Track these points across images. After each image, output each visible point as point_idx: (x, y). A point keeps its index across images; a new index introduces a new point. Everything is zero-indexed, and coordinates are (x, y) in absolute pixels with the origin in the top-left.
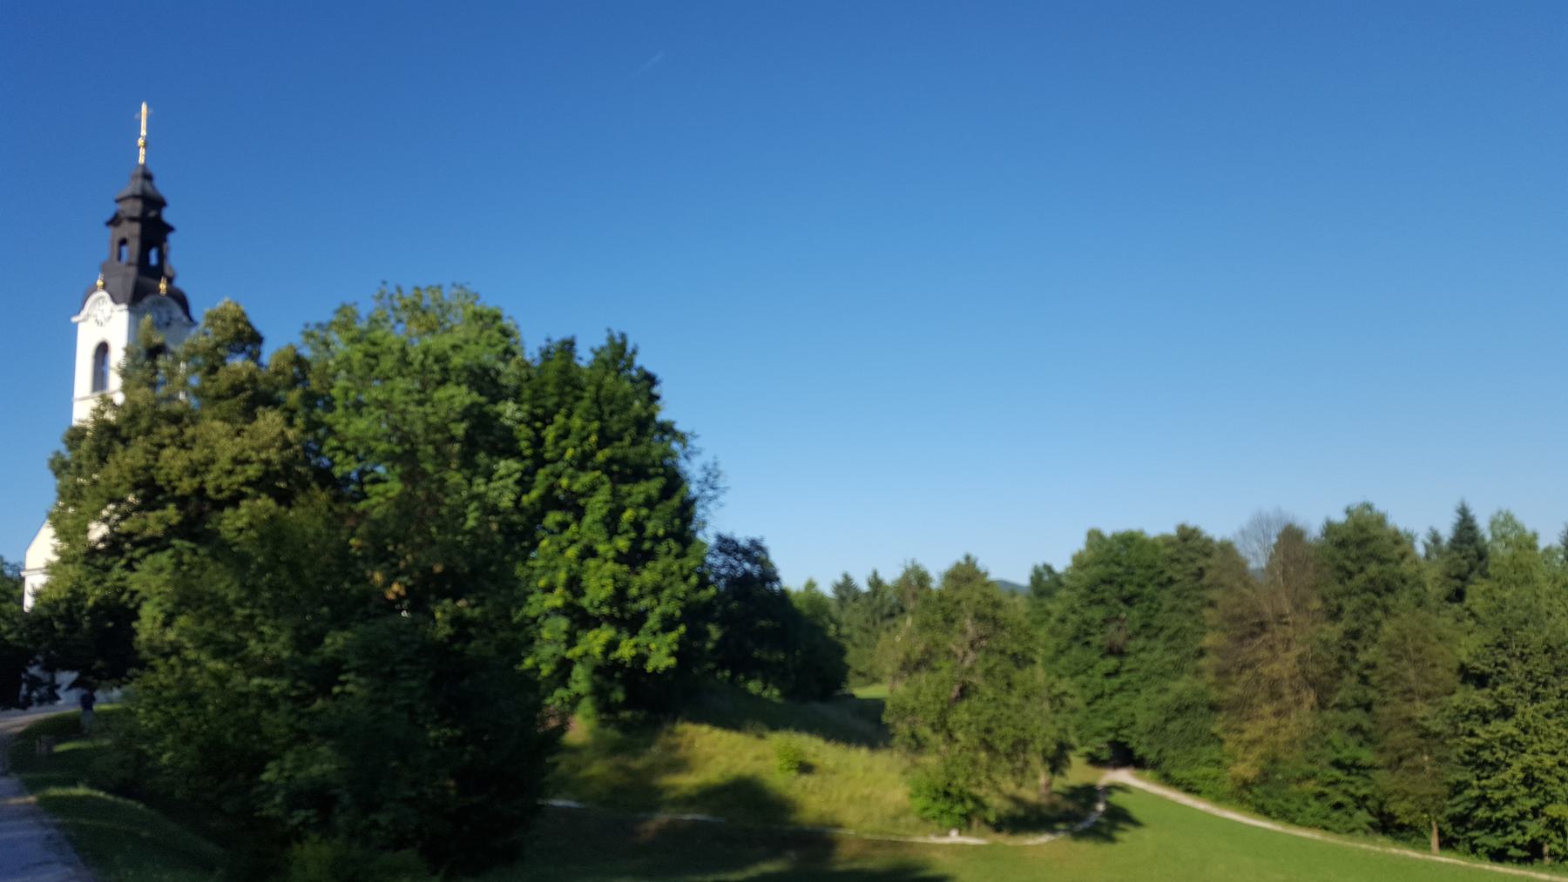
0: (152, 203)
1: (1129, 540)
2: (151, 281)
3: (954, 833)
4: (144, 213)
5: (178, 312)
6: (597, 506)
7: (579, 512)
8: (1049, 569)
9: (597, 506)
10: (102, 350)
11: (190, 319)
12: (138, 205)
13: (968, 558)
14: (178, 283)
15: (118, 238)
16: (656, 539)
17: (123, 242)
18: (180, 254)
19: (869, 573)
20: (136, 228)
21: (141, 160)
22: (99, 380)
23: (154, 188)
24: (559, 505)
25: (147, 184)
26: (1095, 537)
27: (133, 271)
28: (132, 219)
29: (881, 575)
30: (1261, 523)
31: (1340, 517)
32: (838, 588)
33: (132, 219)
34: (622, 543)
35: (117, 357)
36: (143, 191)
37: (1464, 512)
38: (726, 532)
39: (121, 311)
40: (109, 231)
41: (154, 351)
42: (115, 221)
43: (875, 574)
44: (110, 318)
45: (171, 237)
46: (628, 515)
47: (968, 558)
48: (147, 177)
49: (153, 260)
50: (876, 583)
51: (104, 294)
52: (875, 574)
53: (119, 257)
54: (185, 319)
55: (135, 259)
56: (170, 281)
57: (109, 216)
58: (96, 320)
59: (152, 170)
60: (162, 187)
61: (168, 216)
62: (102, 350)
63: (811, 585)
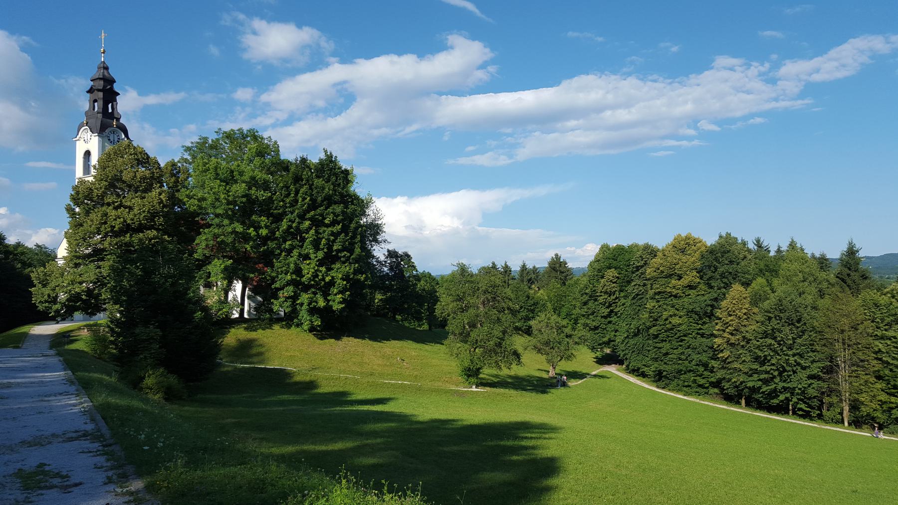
0: (109, 81)
1: (620, 250)
3: (474, 387)
4: (104, 87)
5: (123, 136)
6: (311, 235)
7: (303, 240)
9: (311, 235)
10: (88, 154)
12: (102, 82)
13: (557, 255)
14: (122, 121)
16: (338, 251)
17: (95, 101)
20: (101, 94)
21: (103, 60)
22: (87, 169)
23: (109, 74)
24: (294, 237)
25: (105, 71)
26: (605, 248)
27: (100, 116)
29: (507, 264)
33: (99, 90)
34: (320, 255)
35: (94, 160)
36: (104, 75)
37: (792, 240)
38: (391, 247)
40: (88, 95)
42: (91, 91)
43: (506, 263)
44: (90, 139)
45: (117, 97)
46: (323, 241)
47: (557, 255)
48: (106, 68)
49: (110, 111)
51: (87, 127)
52: (506, 263)
53: (94, 109)
54: (126, 139)
55: (101, 110)
56: (118, 119)
58: (84, 140)
59: (108, 64)
60: (113, 73)
61: (116, 88)
62: (88, 154)
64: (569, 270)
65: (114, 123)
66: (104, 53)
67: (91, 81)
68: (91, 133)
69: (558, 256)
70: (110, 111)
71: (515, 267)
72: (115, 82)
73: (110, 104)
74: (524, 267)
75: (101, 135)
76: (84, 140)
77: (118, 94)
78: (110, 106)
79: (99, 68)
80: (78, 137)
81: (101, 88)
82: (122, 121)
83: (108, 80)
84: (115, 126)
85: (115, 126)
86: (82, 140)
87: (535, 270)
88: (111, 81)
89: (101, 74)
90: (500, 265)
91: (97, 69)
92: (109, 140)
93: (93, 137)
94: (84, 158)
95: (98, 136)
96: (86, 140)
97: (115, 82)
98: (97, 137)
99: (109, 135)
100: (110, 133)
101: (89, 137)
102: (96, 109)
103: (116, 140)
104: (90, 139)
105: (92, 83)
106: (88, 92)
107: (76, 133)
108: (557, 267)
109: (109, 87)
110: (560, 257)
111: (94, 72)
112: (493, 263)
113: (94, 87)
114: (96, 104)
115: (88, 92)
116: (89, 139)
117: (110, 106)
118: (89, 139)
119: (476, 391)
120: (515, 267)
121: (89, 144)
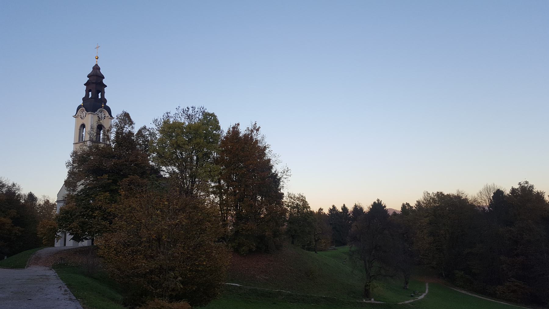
5: (108, 115)
8: (408, 204)
10: (83, 126)
11: (111, 116)
13: (378, 200)
14: (107, 104)
17: (90, 91)
18: (109, 94)
19: (342, 205)
25: (98, 71)
28: (93, 83)
31: (517, 186)
32: (331, 210)
33: (93, 83)
35: (88, 128)
39: (89, 114)
40: (86, 87)
41: (100, 127)
43: (344, 205)
44: (85, 116)
45: (105, 88)
47: (378, 200)
49: (100, 97)
50: (344, 208)
52: (344, 205)
53: (89, 95)
54: (110, 116)
58: (81, 117)
61: (105, 81)
62: (83, 126)
63: (321, 209)
64: (386, 211)
65: (103, 106)
66: (97, 59)
67: (88, 77)
68: (85, 111)
70: (100, 97)
71: (350, 208)
73: (100, 93)
75: (93, 113)
76: (81, 117)
77: (107, 86)
78: (100, 94)
79: (94, 68)
80: (77, 115)
82: (107, 104)
83: (100, 76)
84: (103, 107)
85: (103, 107)
86: (80, 117)
88: (101, 77)
89: (95, 72)
91: (92, 70)
93: (87, 115)
94: (80, 130)
95: (91, 114)
96: (82, 117)
98: (90, 115)
99: (98, 114)
100: (99, 112)
102: (90, 97)
103: (103, 117)
104: (85, 116)
105: (88, 79)
106: (85, 85)
107: (75, 114)
109: (100, 81)
110: (381, 202)
111: (90, 70)
112: (333, 206)
114: (90, 93)
115: (85, 85)
116: (84, 116)
117: (100, 94)
118: (84, 116)
119: (374, 303)
121: (85, 119)
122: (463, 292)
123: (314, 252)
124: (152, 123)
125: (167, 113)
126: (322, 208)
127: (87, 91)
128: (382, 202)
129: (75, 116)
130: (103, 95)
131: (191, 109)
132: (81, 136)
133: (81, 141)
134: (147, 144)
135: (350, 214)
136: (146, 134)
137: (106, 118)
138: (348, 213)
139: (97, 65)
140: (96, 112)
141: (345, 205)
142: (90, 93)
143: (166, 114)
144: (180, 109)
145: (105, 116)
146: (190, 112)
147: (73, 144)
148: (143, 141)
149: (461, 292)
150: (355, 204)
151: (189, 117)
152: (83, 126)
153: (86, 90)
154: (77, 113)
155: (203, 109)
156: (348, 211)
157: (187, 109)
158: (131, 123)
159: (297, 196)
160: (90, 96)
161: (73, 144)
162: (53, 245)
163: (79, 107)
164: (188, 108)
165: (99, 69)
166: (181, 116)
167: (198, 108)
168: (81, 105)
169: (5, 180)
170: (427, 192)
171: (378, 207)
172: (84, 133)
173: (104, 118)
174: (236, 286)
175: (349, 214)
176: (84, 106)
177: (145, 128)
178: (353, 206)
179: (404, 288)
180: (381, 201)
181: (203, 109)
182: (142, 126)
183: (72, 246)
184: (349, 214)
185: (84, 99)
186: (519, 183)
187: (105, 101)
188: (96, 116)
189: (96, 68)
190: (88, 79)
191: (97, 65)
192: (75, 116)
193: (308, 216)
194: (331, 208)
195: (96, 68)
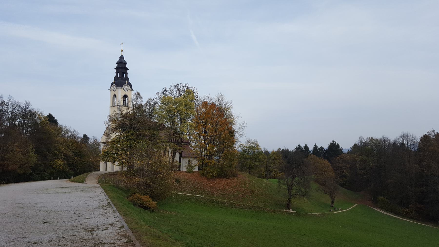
2: (124, 81)
3: (291, 210)
5: (130, 88)
10: (115, 96)
11: (132, 89)
13: (333, 141)
15: (118, 72)
17: (118, 73)
19: (305, 145)
25: (123, 59)
28: (120, 68)
30: (403, 136)
39: (118, 88)
40: (116, 70)
43: (306, 145)
44: (116, 89)
45: (128, 71)
47: (333, 141)
49: (125, 77)
50: (306, 148)
52: (306, 145)
54: (131, 89)
57: (115, 68)
58: (114, 90)
60: (126, 60)
61: (127, 66)
62: (115, 96)
64: (341, 150)
66: (122, 51)
67: (117, 64)
69: (334, 142)
72: (127, 64)
73: (125, 74)
74: (315, 148)
76: (114, 90)
77: (128, 69)
78: (124, 74)
81: (121, 67)
82: (129, 81)
86: (113, 90)
87: (322, 148)
90: (303, 146)
92: (124, 90)
93: (117, 89)
94: (113, 98)
97: (127, 64)
99: (124, 88)
100: (124, 87)
101: (116, 89)
102: (119, 77)
103: (127, 89)
105: (117, 65)
106: (115, 69)
108: (334, 147)
111: (118, 59)
112: (299, 145)
113: (118, 67)
114: (119, 74)
115: (115, 69)
117: (124, 74)
120: (311, 148)
122: (381, 211)
123: (266, 179)
124: (156, 95)
125: (165, 88)
126: (280, 148)
127: (117, 73)
128: (336, 143)
129: (110, 90)
130: (126, 75)
131: (179, 85)
132: (114, 102)
133: (114, 105)
134: (153, 109)
135: (311, 151)
136: (152, 103)
137: (129, 90)
138: (309, 151)
139: (122, 55)
140: (122, 87)
141: (307, 145)
142: (119, 74)
143: (164, 89)
144: (173, 85)
145: (128, 89)
146: (179, 87)
147: (110, 107)
148: (149, 107)
149: (381, 211)
150: (315, 145)
151: (179, 90)
152: (115, 96)
153: (116, 73)
154: (111, 88)
155: (187, 85)
156: (309, 149)
157: (177, 85)
158: (141, 98)
159: (253, 141)
160: (119, 77)
161: (110, 107)
162: (99, 170)
163: (112, 84)
164: (177, 84)
165: (124, 58)
166: (173, 90)
167: (184, 85)
168: (113, 82)
169: (69, 128)
170: (362, 137)
171: (334, 147)
172: (116, 100)
173: (128, 90)
174: (200, 197)
175: (310, 152)
176: (115, 83)
177: (151, 99)
178: (313, 146)
179: (331, 206)
180: (336, 142)
181: (187, 85)
182: (149, 98)
183: (110, 171)
184: (310, 152)
185: (116, 78)
186: (428, 131)
187: (128, 79)
188: (123, 89)
189: (122, 58)
190: (117, 65)
191: (122, 55)
192: (110, 90)
193: (259, 155)
194: (298, 146)
195: (122, 58)
